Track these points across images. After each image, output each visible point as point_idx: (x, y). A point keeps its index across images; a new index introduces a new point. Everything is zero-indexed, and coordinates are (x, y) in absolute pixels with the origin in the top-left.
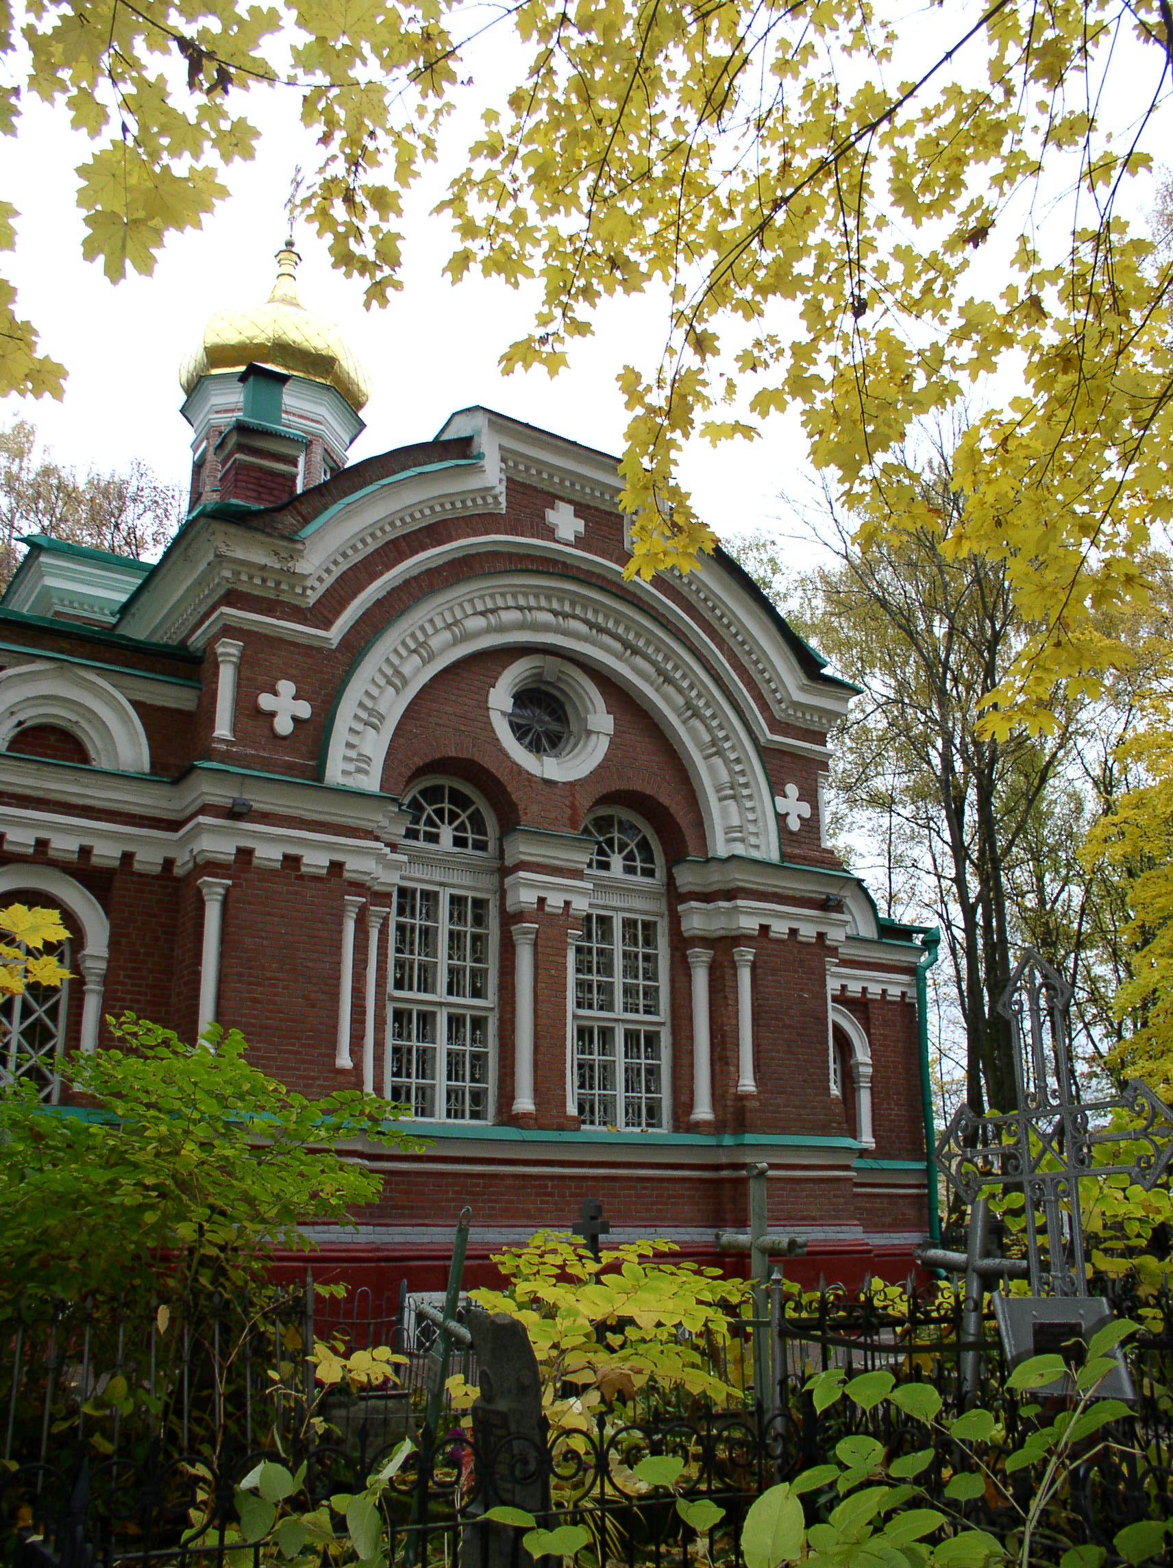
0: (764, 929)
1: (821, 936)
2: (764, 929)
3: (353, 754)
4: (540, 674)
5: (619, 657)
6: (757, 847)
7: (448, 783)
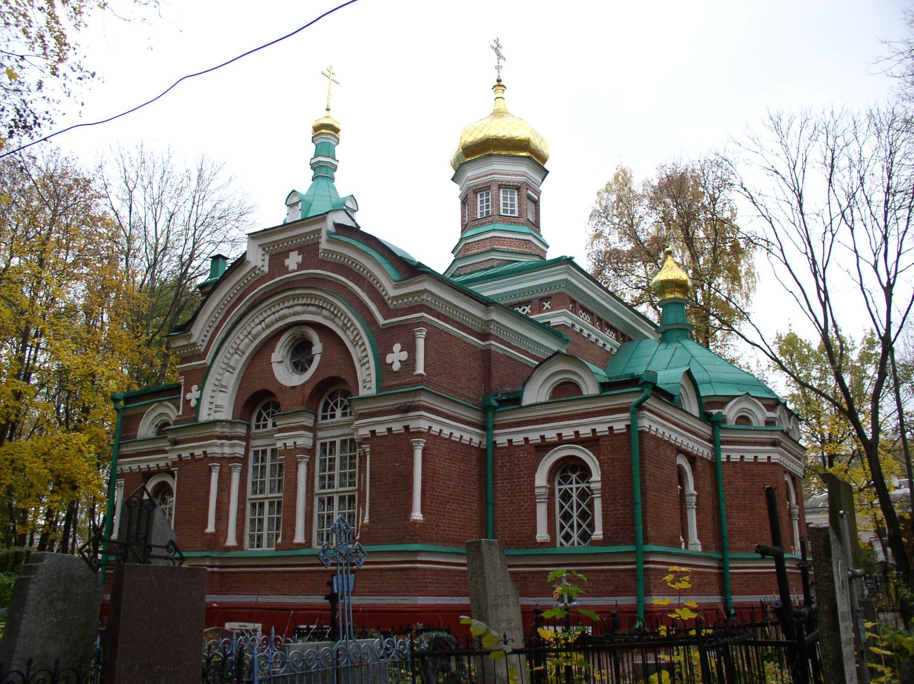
0: (373, 432)
1: (407, 428)
3: (213, 406)
4: (294, 337)
5: (318, 314)
7: (259, 401)
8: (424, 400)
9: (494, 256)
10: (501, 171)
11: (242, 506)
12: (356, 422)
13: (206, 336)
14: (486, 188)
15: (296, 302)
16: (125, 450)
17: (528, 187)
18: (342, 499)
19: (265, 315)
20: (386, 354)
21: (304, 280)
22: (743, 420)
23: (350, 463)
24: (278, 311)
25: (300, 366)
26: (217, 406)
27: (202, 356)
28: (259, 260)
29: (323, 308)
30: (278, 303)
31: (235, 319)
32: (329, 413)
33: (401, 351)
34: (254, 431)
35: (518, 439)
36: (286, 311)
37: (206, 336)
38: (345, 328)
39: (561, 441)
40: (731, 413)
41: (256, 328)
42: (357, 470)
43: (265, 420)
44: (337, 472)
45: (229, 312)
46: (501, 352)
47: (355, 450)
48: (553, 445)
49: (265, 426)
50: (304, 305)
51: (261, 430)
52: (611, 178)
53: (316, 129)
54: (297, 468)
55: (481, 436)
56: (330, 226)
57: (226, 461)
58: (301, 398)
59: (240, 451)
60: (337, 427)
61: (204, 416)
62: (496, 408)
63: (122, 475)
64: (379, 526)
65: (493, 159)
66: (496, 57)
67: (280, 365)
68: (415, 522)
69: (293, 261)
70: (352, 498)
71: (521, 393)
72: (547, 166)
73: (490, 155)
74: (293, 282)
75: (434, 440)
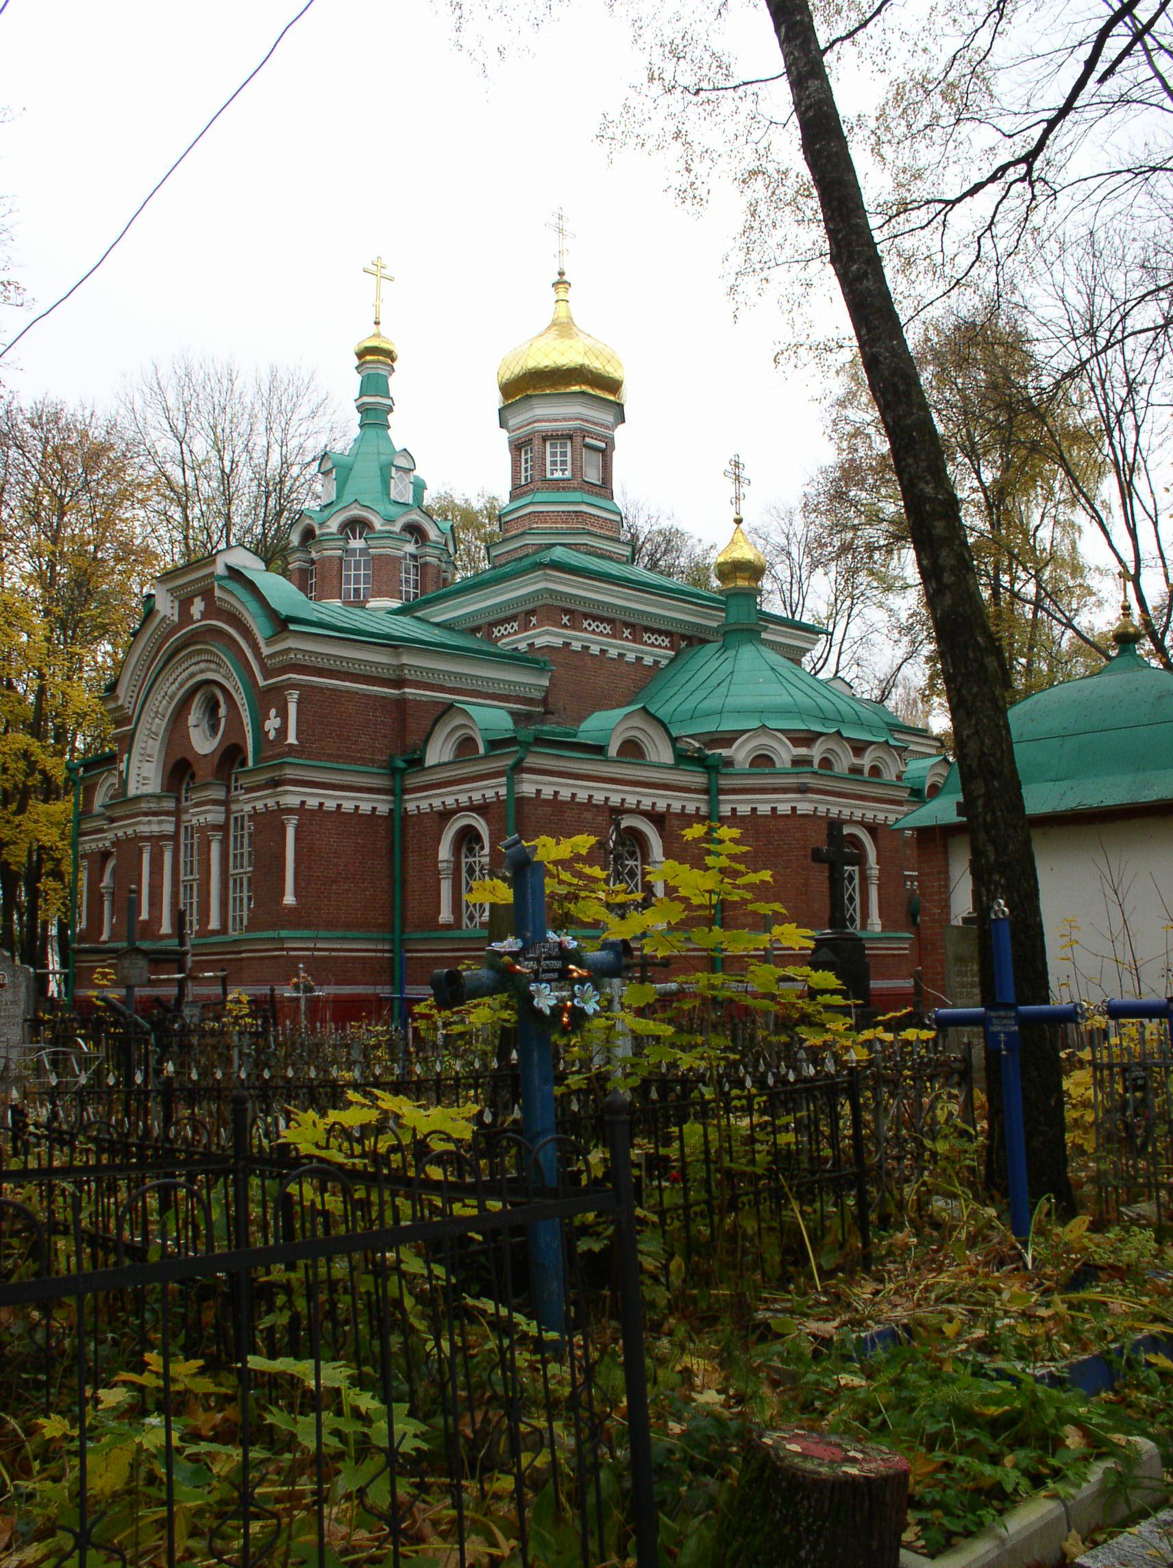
7: (180, 772)
8: (290, 773)
9: (528, 540)
10: (563, 408)
16: (86, 826)
22: (763, 761)
35: (424, 805)
39: (460, 809)
40: (740, 753)
41: (171, 687)
48: (460, 809)
53: (361, 355)
56: (220, 569)
57: (156, 840)
59: (169, 828)
61: (132, 791)
63: (84, 857)
65: (534, 401)
68: (286, 907)
69: (198, 607)
71: (424, 751)
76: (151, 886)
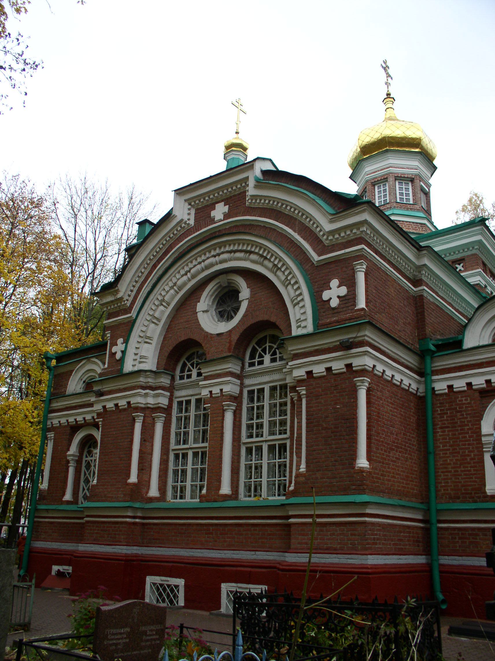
0: (310, 373)
1: (349, 366)
2: (310, 373)
3: (138, 357)
4: (221, 286)
5: (245, 260)
6: (305, 327)
7: (183, 351)
11: (165, 457)
12: (290, 364)
13: (132, 291)
14: (384, 180)
15: (222, 250)
17: (421, 179)
18: (271, 448)
19: (191, 266)
20: (322, 291)
21: (231, 228)
23: (281, 411)
24: (204, 261)
25: (225, 315)
26: (142, 357)
27: (128, 310)
28: (186, 215)
29: (251, 252)
30: (204, 252)
31: (160, 272)
32: (257, 360)
33: (339, 287)
34: (178, 381)
35: (460, 385)
36: (212, 260)
37: (132, 291)
38: (275, 269)
41: (183, 278)
42: (288, 417)
43: (190, 370)
44: (266, 420)
45: (155, 266)
46: (431, 300)
47: (286, 396)
49: (189, 376)
50: (230, 252)
51: (186, 380)
52: (466, 202)
54: (223, 416)
55: (419, 382)
56: (257, 173)
57: (150, 412)
58: (228, 345)
59: (164, 401)
60: (266, 373)
61: (128, 367)
62: (434, 352)
63: (52, 429)
64: (318, 475)
65: (389, 155)
66: (385, 75)
67: (205, 315)
68: (361, 470)
69: (220, 211)
70: (283, 447)
72: (435, 162)
73: (387, 151)
74: (220, 231)
75: (379, 383)
76: (141, 452)
